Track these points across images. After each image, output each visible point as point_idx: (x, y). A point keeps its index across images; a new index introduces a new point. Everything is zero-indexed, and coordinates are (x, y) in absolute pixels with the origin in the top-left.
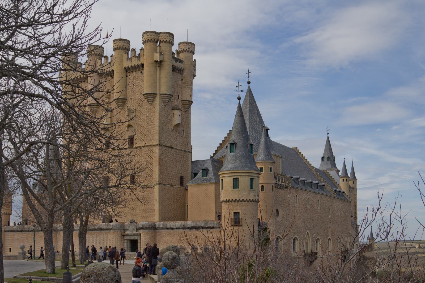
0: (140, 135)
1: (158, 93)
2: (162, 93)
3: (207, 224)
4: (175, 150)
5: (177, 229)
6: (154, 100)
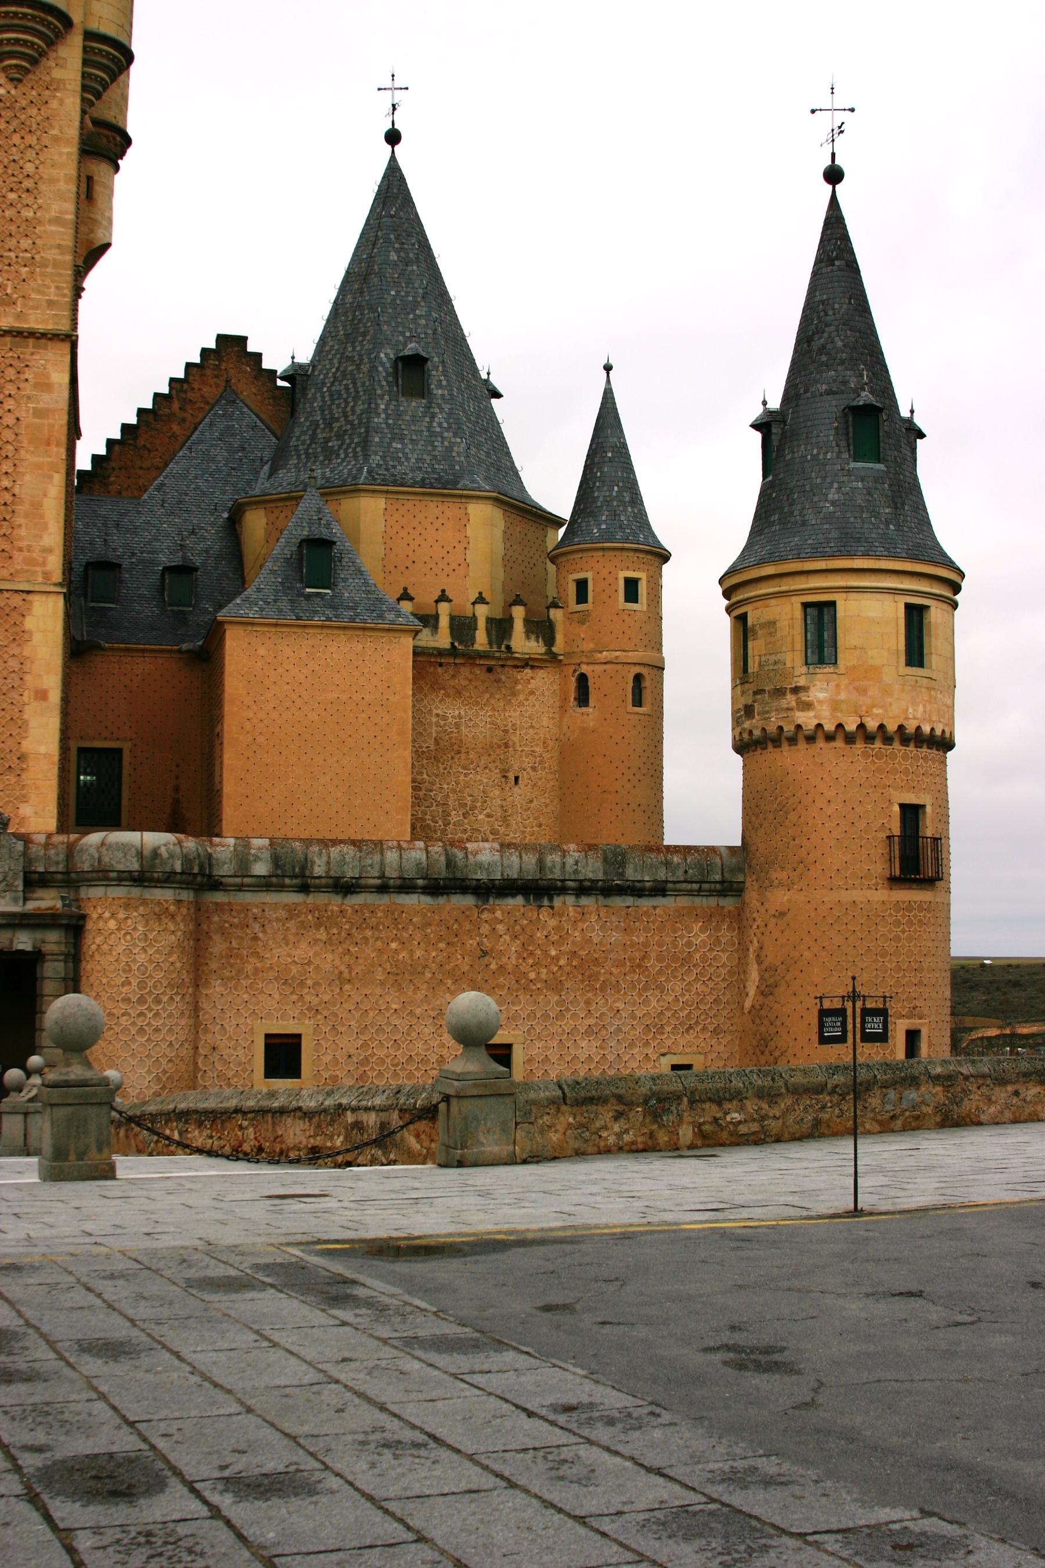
1: (77, 17)
2: (94, 26)
3: (623, 864)
5: (383, 889)
6: (43, 54)
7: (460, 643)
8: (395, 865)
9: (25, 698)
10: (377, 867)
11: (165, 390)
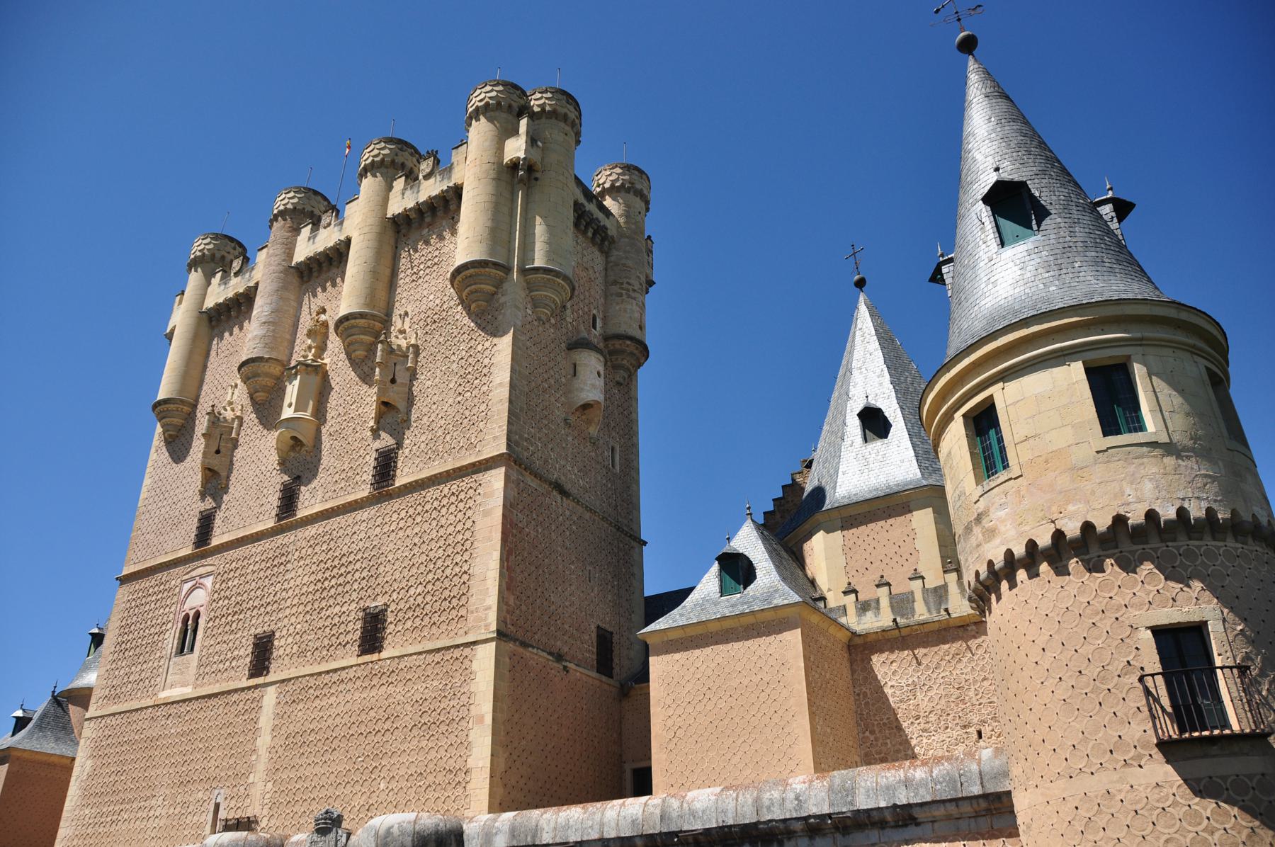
0: (423, 438)
4: (580, 510)
6: (496, 293)
7: (902, 616)
8: (613, 824)
9: (470, 725)
10: (596, 827)
11: (771, 508)
